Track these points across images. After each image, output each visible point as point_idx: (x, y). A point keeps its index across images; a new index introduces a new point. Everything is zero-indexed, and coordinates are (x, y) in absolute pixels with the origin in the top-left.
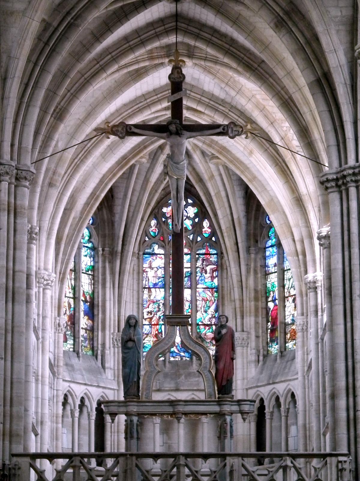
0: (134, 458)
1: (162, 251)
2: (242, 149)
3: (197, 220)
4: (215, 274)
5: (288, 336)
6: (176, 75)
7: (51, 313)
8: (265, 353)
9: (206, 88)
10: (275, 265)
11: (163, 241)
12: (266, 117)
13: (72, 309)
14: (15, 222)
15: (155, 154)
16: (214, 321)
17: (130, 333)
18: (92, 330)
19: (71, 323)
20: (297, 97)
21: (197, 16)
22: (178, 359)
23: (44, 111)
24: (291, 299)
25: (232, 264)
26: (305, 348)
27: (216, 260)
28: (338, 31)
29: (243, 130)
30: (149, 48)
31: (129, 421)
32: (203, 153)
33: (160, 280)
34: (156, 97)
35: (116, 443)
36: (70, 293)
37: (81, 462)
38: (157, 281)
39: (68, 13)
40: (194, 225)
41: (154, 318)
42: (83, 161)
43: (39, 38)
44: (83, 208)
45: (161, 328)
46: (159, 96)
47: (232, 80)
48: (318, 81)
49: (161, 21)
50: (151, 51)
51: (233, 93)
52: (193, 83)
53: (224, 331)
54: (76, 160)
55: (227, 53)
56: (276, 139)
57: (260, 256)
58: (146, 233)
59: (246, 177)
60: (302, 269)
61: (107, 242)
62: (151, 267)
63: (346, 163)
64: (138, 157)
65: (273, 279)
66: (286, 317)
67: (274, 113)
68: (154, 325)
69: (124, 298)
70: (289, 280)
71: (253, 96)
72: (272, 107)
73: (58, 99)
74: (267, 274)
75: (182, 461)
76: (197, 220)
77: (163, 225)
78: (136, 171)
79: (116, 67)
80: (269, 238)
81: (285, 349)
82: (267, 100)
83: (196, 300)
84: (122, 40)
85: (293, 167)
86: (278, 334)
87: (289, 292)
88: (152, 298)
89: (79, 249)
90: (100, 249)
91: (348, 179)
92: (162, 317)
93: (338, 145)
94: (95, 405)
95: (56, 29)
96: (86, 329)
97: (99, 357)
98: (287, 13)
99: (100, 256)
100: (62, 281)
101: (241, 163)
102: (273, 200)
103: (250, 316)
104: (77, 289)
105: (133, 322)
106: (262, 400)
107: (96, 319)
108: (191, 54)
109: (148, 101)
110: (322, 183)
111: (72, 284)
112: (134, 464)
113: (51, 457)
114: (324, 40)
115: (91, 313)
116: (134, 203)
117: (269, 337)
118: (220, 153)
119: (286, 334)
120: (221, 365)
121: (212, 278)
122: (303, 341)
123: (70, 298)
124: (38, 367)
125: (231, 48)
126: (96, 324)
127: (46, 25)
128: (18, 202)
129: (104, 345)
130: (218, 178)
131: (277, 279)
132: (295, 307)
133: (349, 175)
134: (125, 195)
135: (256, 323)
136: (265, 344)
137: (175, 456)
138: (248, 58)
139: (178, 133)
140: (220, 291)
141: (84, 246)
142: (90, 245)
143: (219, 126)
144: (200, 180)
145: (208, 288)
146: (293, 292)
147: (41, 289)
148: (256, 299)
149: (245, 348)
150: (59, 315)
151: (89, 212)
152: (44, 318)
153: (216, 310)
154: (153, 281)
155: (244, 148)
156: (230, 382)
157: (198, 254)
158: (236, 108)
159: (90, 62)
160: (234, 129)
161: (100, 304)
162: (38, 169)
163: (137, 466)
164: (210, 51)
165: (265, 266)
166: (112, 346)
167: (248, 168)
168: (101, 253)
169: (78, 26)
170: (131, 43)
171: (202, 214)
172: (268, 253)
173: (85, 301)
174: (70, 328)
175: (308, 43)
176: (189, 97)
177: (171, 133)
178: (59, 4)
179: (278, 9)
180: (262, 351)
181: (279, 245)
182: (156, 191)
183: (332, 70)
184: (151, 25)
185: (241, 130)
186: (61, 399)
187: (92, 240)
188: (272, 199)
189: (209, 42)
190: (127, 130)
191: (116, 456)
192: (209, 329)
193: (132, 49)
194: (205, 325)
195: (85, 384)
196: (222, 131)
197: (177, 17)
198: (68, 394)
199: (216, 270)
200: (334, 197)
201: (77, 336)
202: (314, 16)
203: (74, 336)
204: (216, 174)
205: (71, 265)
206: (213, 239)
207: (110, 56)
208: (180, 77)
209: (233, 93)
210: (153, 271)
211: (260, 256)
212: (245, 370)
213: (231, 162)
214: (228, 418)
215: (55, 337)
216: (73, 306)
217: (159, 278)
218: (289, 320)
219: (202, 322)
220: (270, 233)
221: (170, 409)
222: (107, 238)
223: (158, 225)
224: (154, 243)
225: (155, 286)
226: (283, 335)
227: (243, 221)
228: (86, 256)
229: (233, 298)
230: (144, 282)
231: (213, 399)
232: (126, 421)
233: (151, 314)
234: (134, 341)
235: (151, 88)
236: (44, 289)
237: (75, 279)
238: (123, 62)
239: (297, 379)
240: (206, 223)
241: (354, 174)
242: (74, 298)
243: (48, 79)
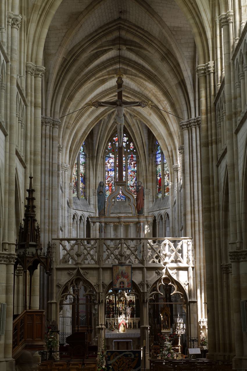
0: (103, 240)
1: (113, 156)
2: (147, 113)
3: (128, 143)
5: (166, 190)
6: (120, 81)
7: (67, 182)
8: (156, 197)
9: (132, 87)
10: (160, 161)
11: (114, 152)
12: (157, 99)
13: (76, 180)
14: (52, 143)
15: (110, 115)
16: (135, 184)
17: (101, 189)
18: (84, 188)
19: (76, 186)
20: (169, 90)
21: (128, 57)
22: (120, 200)
23: (64, 97)
24: (167, 175)
25: (143, 161)
26: (173, 195)
27: (136, 159)
28: (187, 62)
29: (147, 104)
30: (108, 70)
31: (101, 225)
32: (130, 115)
33: (112, 168)
34: (111, 91)
35: (95, 235)
36: (75, 173)
37: (81, 242)
38: (111, 168)
39: (74, 55)
40: (126, 145)
41: (110, 184)
42: (80, 118)
43: (62, 65)
44: (80, 138)
45: (113, 188)
46: (112, 91)
47: (142, 84)
48: (179, 83)
49: (113, 58)
50: (108, 72)
51: (143, 89)
52: (126, 85)
53: (140, 188)
54: (77, 118)
55: (141, 72)
56: (161, 108)
57: (154, 158)
58: (107, 148)
59: (148, 124)
60: (172, 163)
61: (90, 152)
62: (108, 162)
63: (191, 117)
64: (104, 116)
65: (159, 167)
66: (165, 183)
67: (160, 97)
68: (110, 186)
70: (166, 167)
71: (151, 90)
72: (159, 95)
73: (70, 92)
74: (157, 165)
75: (123, 241)
76: (128, 143)
77: (113, 145)
78: (102, 122)
79: (94, 78)
80: (158, 150)
81: (164, 196)
82: (157, 92)
83: (128, 176)
84: (97, 66)
85: (168, 120)
86: (161, 190)
87: (166, 173)
88: (109, 175)
89: (79, 155)
90: (88, 155)
91: (192, 124)
93: (188, 110)
94: (86, 219)
95: (69, 61)
96: (82, 188)
97: (88, 200)
98: (166, 54)
99: (88, 158)
100: (72, 168)
101: (146, 118)
102: (159, 134)
103: (150, 182)
104: (78, 171)
105: (102, 184)
106: (155, 217)
107: (86, 184)
108: (125, 72)
109: (107, 93)
110: (181, 126)
111: (76, 170)
112: (103, 243)
113: (69, 240)
114: (182, 66)
115: (84, 181)
116: (101, 136)
117: (158, 191)
118: (138, 115)
119: (165, 190)
120: (139, 202)
121: (134, 167)
122: (172, 193)
123: (76, 175)
124: (62, 204)
125: (142, 70)
126: (86, 185)
127: (65, 60)
128: (54, 135)
129: (89, 196)
130: (136, 125)
131: (161, 167)
132: (169, 179)
133: (192, 122)
134: (98, 133)
135: (152, 185)
137: (120, 239)
138: (150, 74)
139: (120, 105)
140: (137, 172)
141: (81, 154)
142: (83, 153)
143: (137, 102)
144: (129, 126)
145: (132, 171)
146: (168, 172)
147: (64, 171)
148: (152, 176)
149: (148, 196)
150: (71, 182)
151: (83, 139)
152: (65, 183)
153: (136, 180)
154: (109, 168)
155: (147, 113)
156: (142, 208)
157: (128, 157)
158: (144, 95)
159: (83, 76)
160: (144, 104)
161: (88, 178)
162: (62, 121)
163: (104, 243)
164: (134, 71)
165: (156, 162)
166: (93, 195)
167: (149, 121)
168: (88, 156)
169: (78, 60)
170: (100, 68)
171: (130, 140)
172: (157, 157)
173: (82, 177)
174: (76, 187)
175: (175, 67)
176: (125, 91)
177: (117, 106)
178: (70, 51)
179: (162, 53)
180: (155, 197)
181: (162, 153)
182: (111, 131)
183: (185, 78)
184: (109, 60)
185: (147, 104)
186: (72, 217)
187: (84, 151)
188: (159, 134)
189: (133, 67)
190: (99, 104)
191: (96, 239)
192: (133, 188)
193: (101, 70)
194: (131, 186)
195: (82, 211)
196: (139, 104)
197: (120, 57)
199: (135, 164)
200: (186, 133)
202: (178, 55)
203: (77, 191)
204: (136, 123)
205: (76, 162)
206: (135, 151)
207: (91, 73)
208: (121, 82)
209: (143, 89)
211: (154, 158)
212: (148, 205)
213: (142, 118)
214: (142, 224)
215: (69, 191)
216: (76, 179)
217: (112, 167)
218: (166, 184)
219: (130, 185)
220: (158, 148)
221: (118, 220)
222: (90, 151)
223: (112, 145)
224: (110, 153)
225: (111, 170)
226: (163, 190)
227: (147, 143)
228: (82, 158)
229: (143, 175)
230: (106, 169)
231: (136, 216)
232: (99, 225)
234: (103, 192)
235: (109, 87)
236: (64, 171)
237: (77, 167)
238: (97, 76)
239: (170, 208)
240: (131, 144)
241: (194, 122)
242: (77, 176)
243: (66, 82)
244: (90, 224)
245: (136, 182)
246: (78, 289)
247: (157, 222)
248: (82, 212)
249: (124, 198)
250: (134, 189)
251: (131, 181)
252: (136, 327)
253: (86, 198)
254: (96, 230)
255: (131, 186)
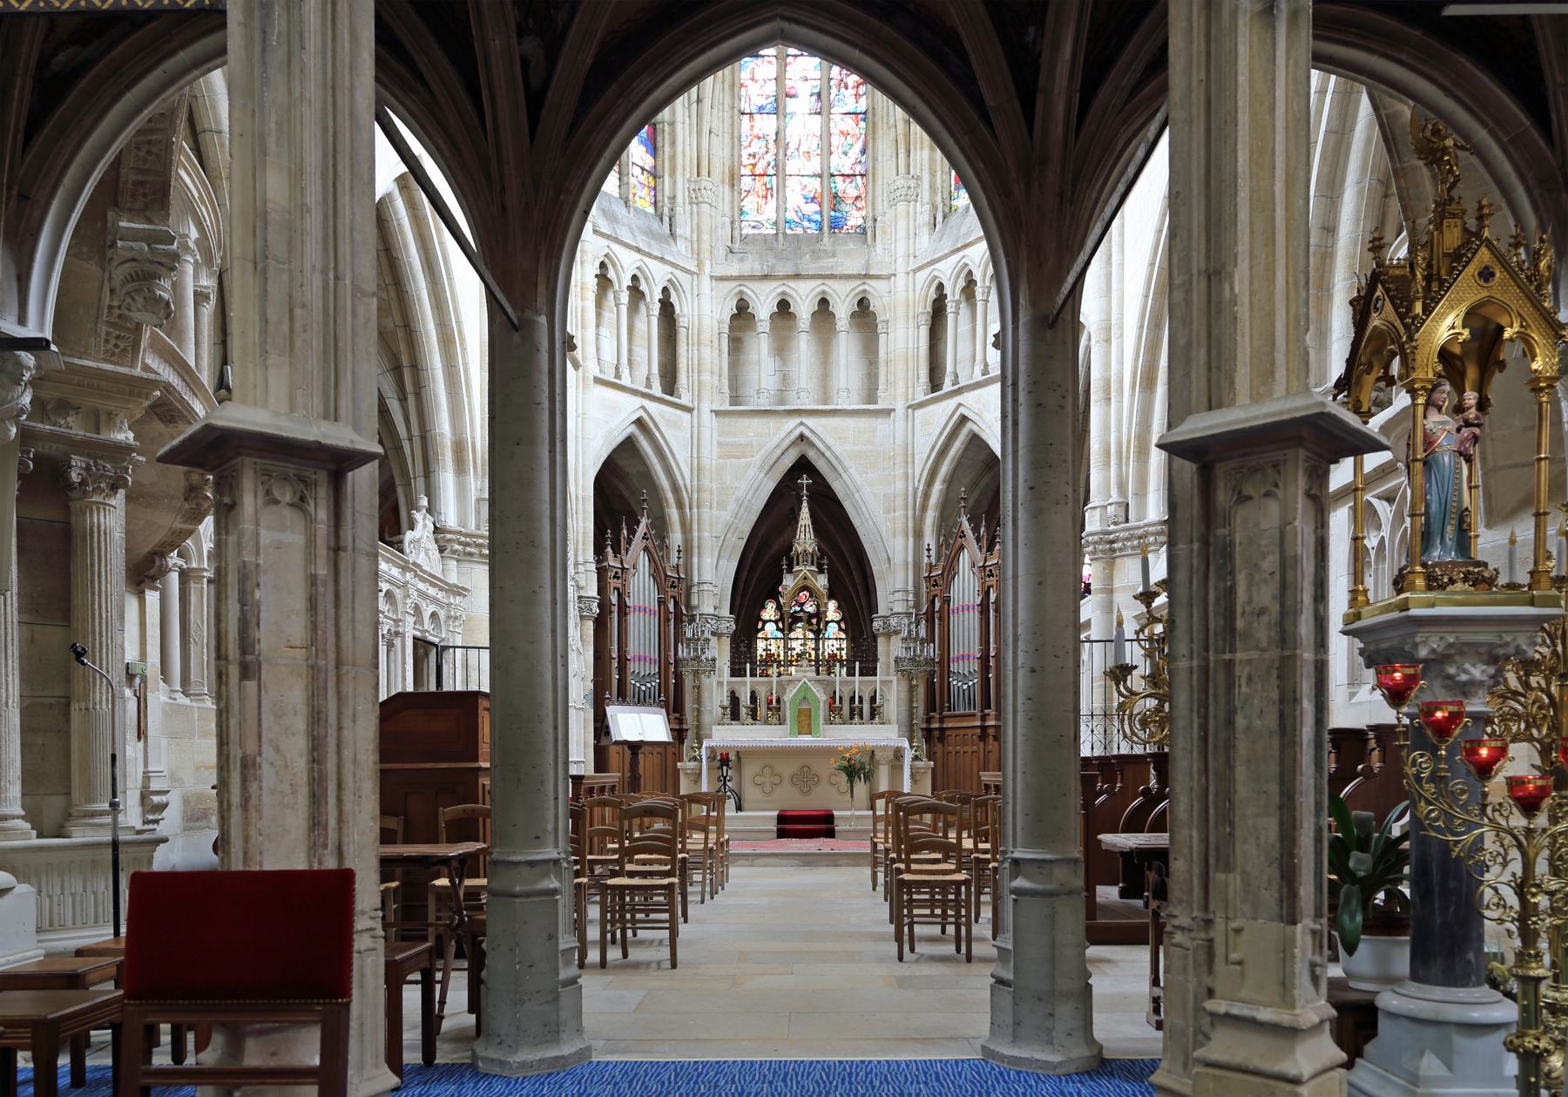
4: (862, 89)
8: (947, 210)
16: (859, 169)
22: (799, 231)
69: (706, 118)
83: (830, 135)
92: (773, 164)
94: (658, 295)
97: (666, 219)
103: (922, 148)
107: (660, 153)
121: (857, 96)
126: (659, 163)
136: (946, 195)
140: (870, 120)
153: (863, 152)
195: (639, 250)
198: (607, 261)
201: (625, 172)
210: (757, 85)
217: (768, 97)
229: (892, 121)
233: (754, 156)
244: (674, 321)
245: (863, 160)
246: (623, 569)
247: (949, 305)
248: (639, 256)
249: (813, 225)
250: (857, 187)
251: (845, 154)
252: (861, 717)
253: (659, 211)
254: (699, 344)
255: (843, 175)
